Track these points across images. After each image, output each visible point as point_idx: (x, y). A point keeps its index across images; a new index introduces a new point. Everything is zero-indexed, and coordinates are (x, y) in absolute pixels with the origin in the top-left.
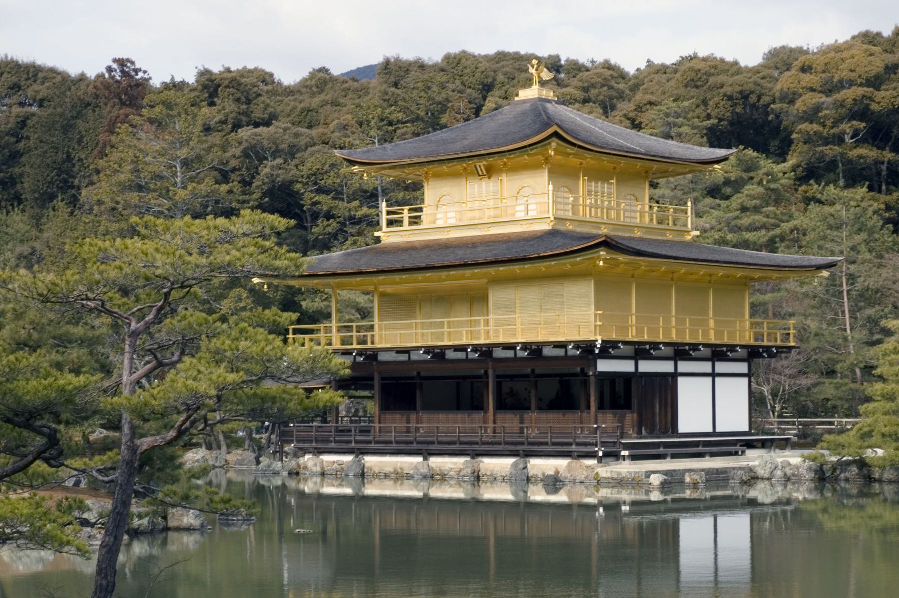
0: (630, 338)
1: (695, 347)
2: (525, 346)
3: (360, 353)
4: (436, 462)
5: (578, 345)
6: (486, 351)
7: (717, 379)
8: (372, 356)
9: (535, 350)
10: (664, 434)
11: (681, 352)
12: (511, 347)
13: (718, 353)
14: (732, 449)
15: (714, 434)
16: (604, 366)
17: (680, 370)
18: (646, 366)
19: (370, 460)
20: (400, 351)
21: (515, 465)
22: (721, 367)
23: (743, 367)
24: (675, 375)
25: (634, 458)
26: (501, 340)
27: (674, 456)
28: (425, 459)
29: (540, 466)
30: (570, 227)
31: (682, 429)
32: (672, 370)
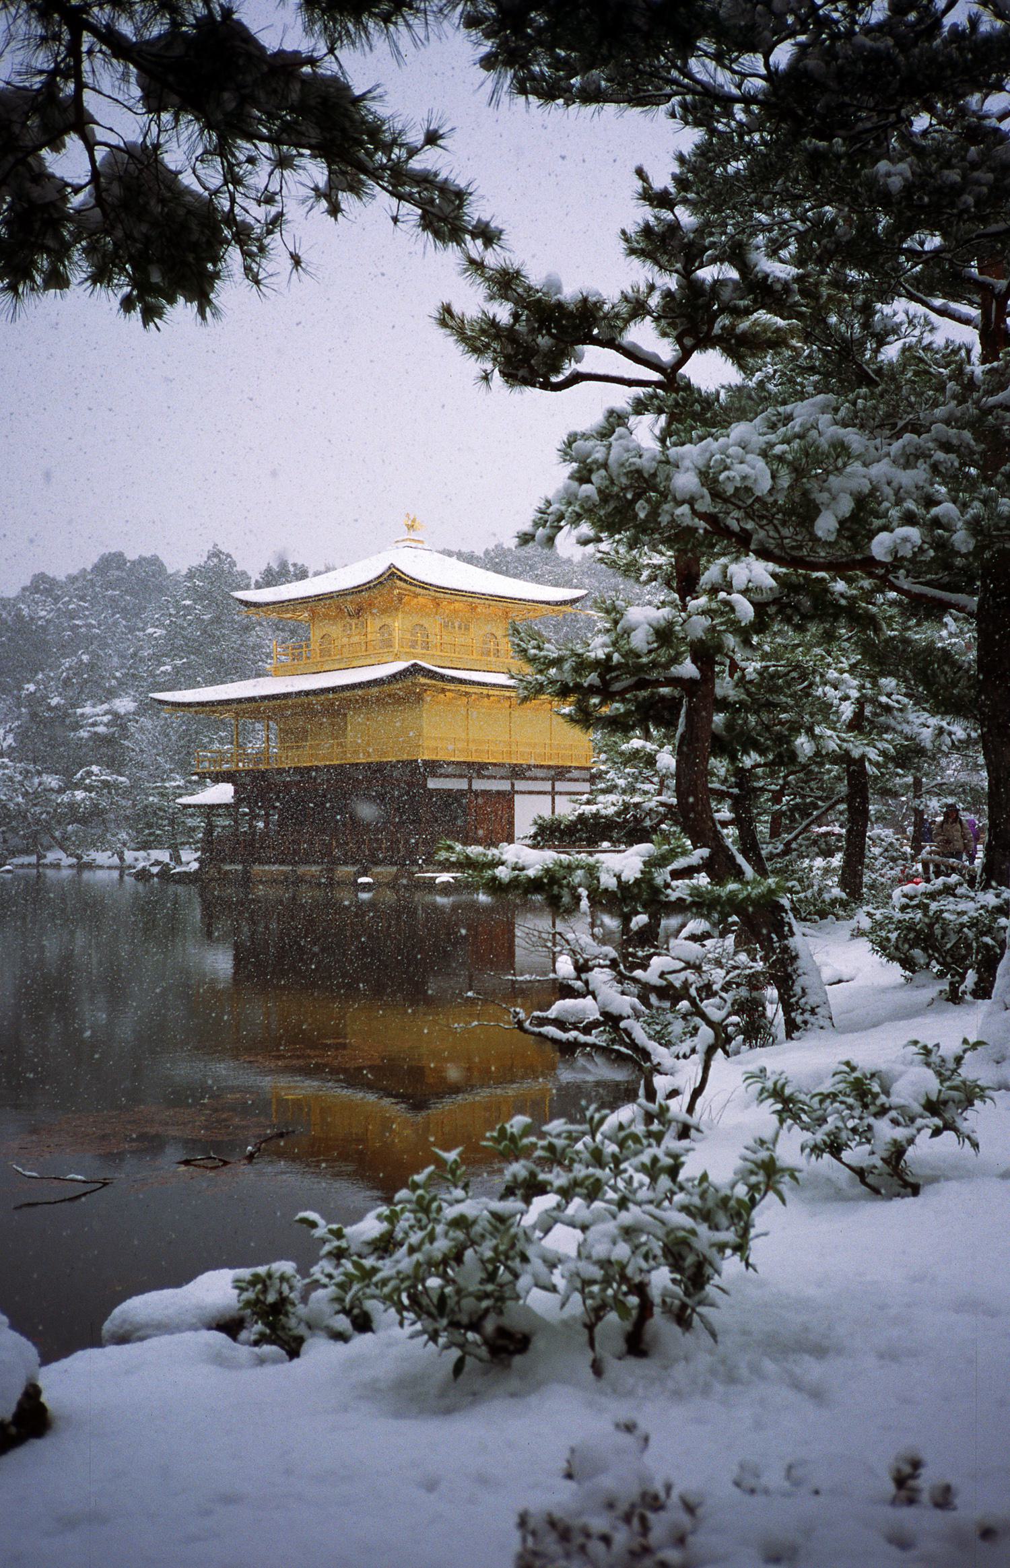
5: (406, 764)
7: (557, 797)
16: (432, 784)
17: (516, 788)
18: (479, 785)
22: (560, 786)
24: (514, 792)
32: (509, 788)
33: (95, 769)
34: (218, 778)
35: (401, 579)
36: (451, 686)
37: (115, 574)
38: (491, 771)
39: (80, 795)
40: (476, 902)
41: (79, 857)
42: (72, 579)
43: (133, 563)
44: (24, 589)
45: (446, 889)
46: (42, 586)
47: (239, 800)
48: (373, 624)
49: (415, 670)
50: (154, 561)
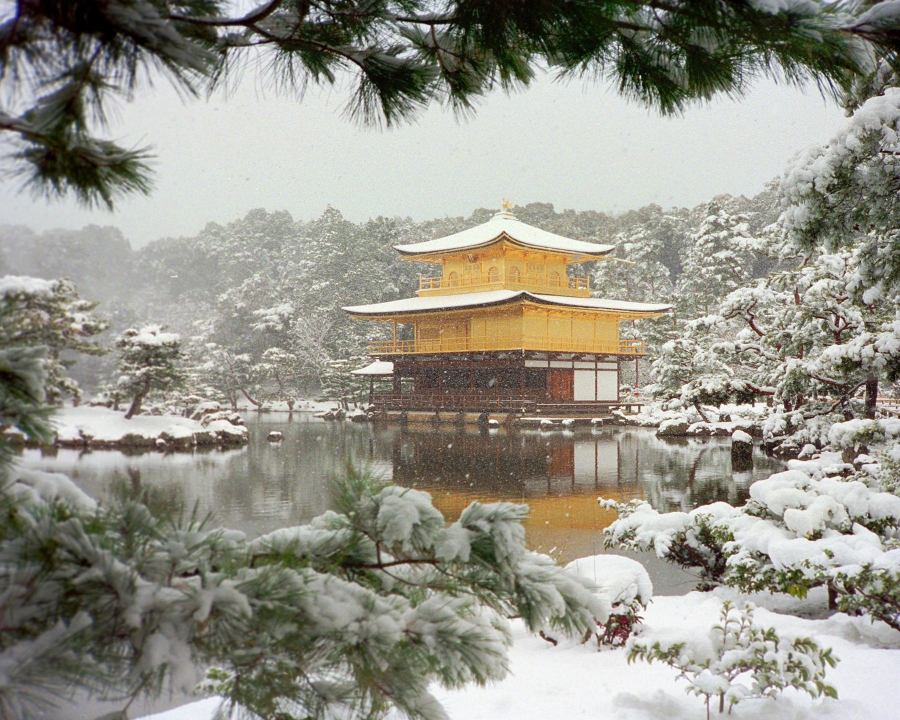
0: (544, 349)
2: (487, 353)
5: (514, 352)
8: (413, 357)
12: (480, 353)
14: (605, 410)
15: (596, 402)
16: (529, 364)
18: (554, 364)
19: (412, 414)
20: (427, 355)
21: (481, 417)
22: (600, 365)
23: (615, 366)
26: (476, 350)
28: (437, 413)
33: (275, 350)
34: (383, 359)
35: (508, 240)
36: (542, 306)
37: (259, 223)
38: (563, 356)
39: (267, 366)
40: (562, 435)
41: (260, 406)
42: (232, 226)
43: (272, 216)
44: (202, 232)
45: (548, 427)
46: (213, 230)
47: (397, 373)
48: (485, 266)
49: (524, 296)
50: (286, 214)
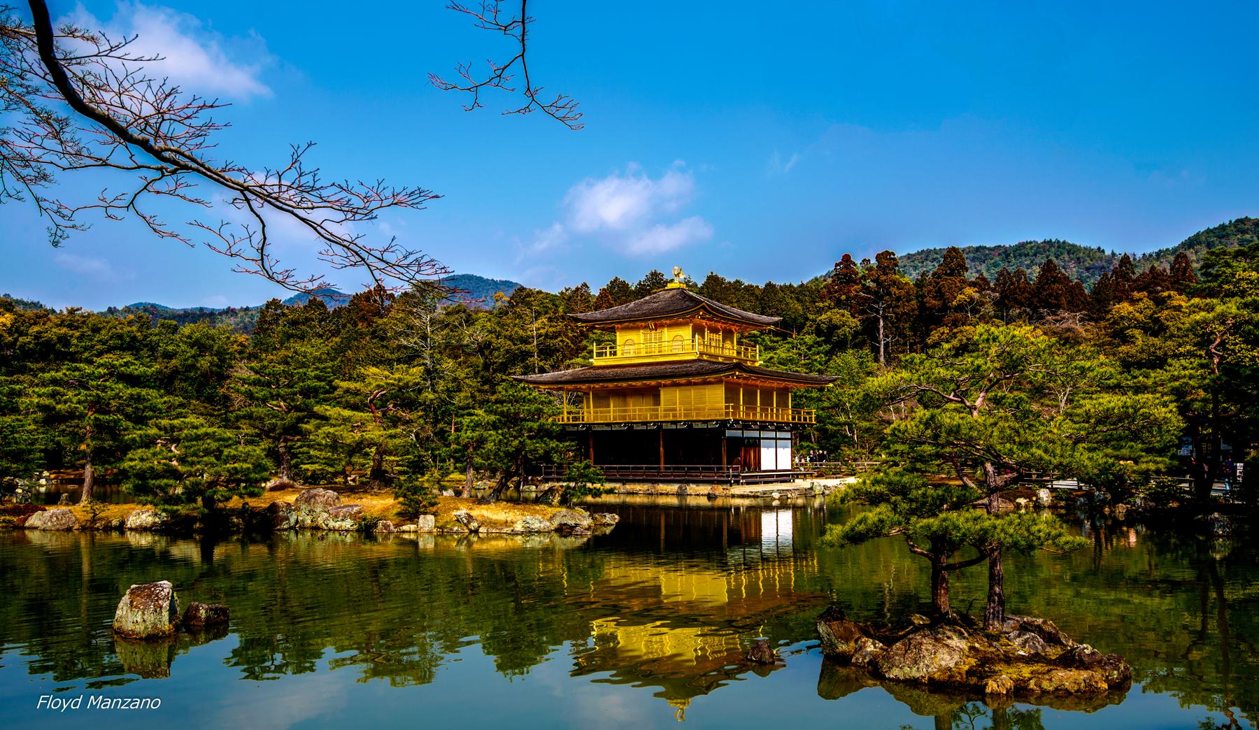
1: (772, 423)
3: (584, 425)
4: (629, 487)
6: (659, 424)
9: (689, 423)
10: (755, 471)
11: (763, 427)
13: (779, 428)
16: (728, 433)
18: (748, 434)
22: (779, 435)
23: (788, 435)
25: (748, 483)
27: (766, 483)
29: (692, 488)
30: (705, 358)
31: (763, 468)
